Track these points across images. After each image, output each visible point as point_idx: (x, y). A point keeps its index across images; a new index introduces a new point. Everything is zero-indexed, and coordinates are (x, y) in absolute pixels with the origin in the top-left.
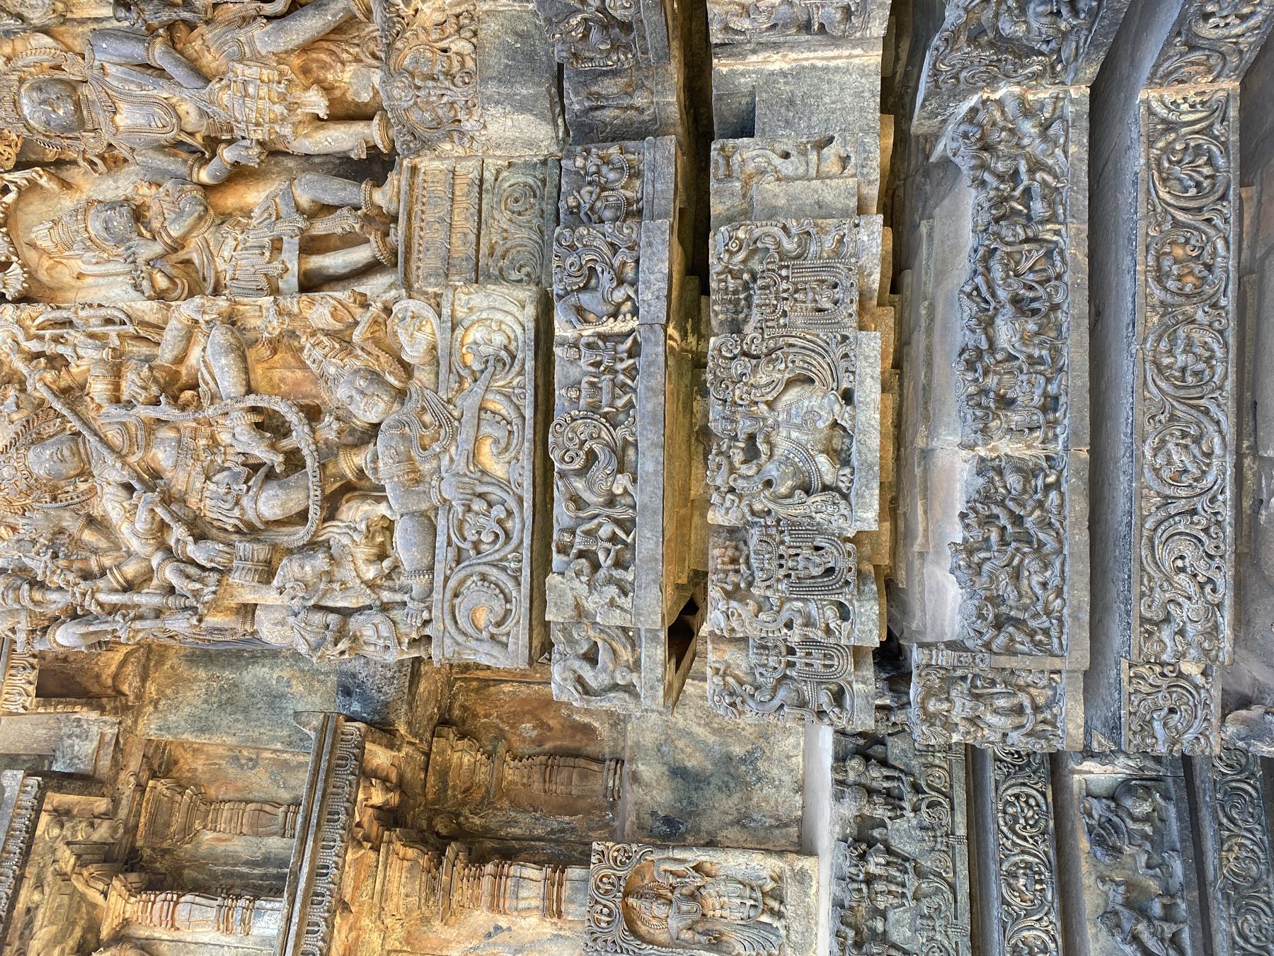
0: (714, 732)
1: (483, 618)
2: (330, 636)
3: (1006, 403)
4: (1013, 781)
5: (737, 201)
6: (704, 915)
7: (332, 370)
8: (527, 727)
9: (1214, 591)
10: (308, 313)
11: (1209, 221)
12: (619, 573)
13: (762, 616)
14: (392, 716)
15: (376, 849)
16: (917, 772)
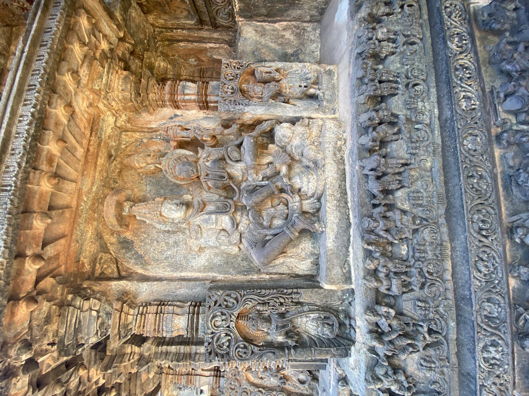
0: (279, 45)
8: (192, 61)
14: (112, 9)
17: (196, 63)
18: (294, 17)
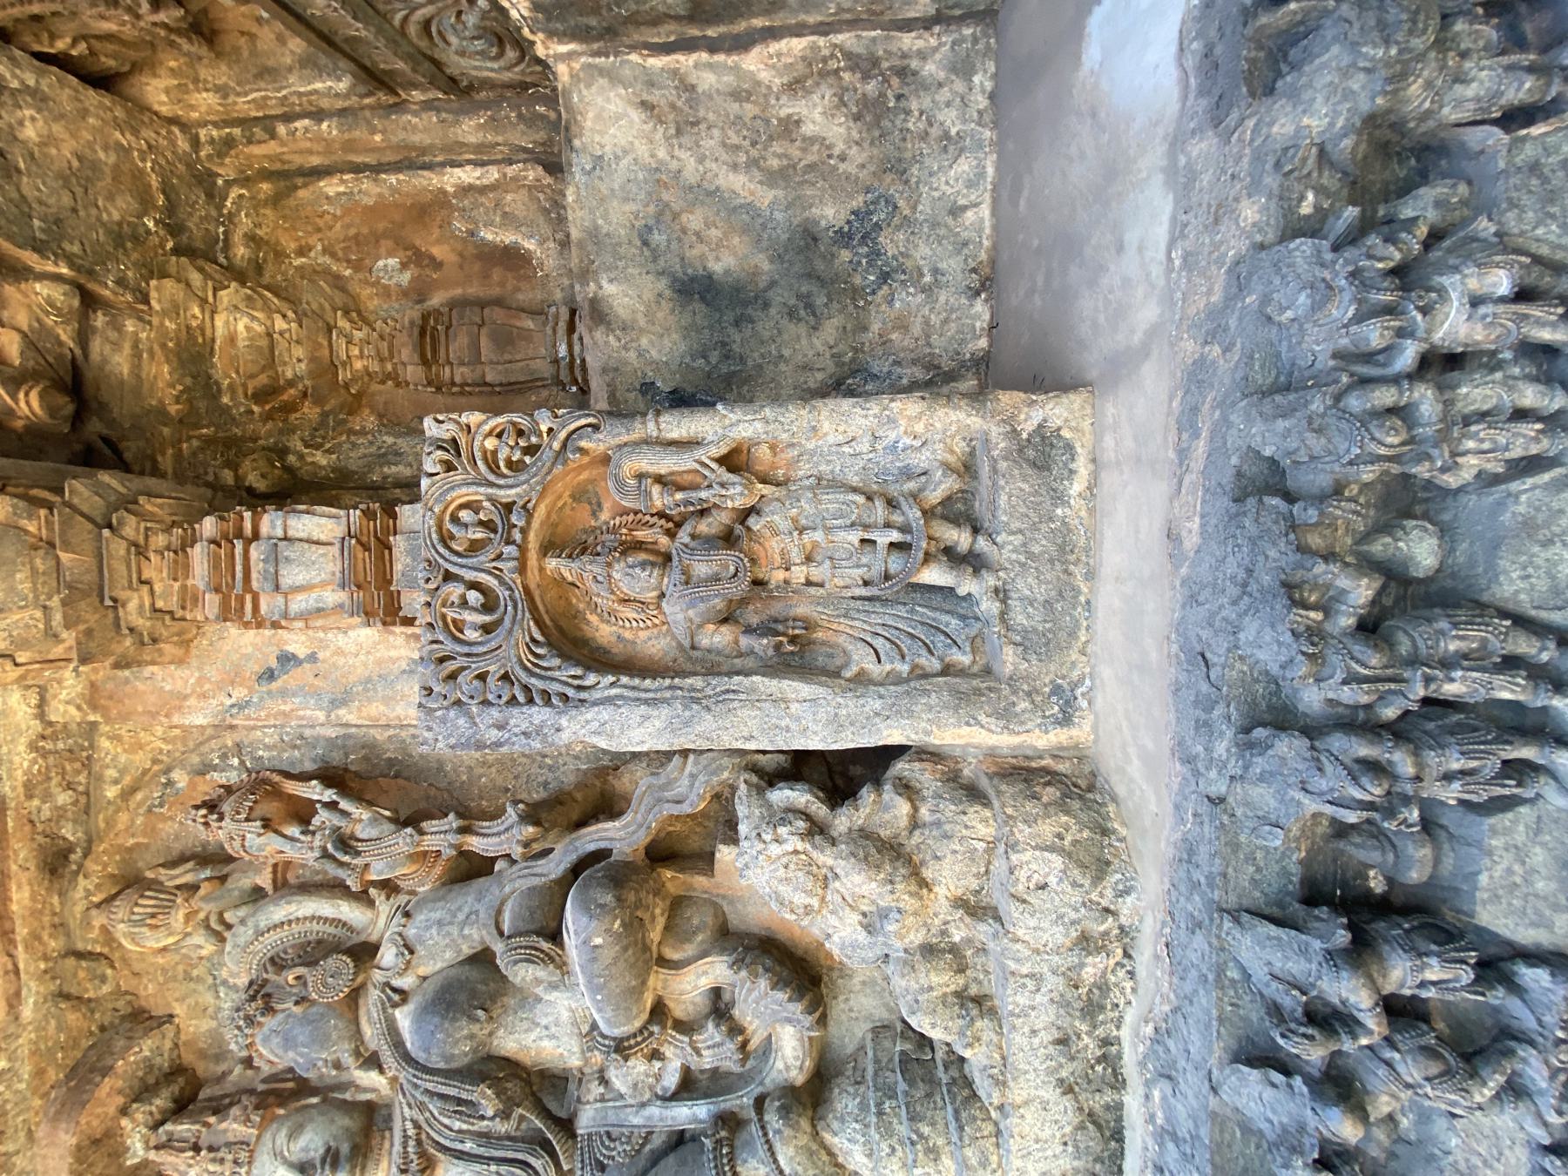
0: (772, 178)
6: (757, 583)
8: (388, 265)
17: (406, 278)
18: (840, 10)
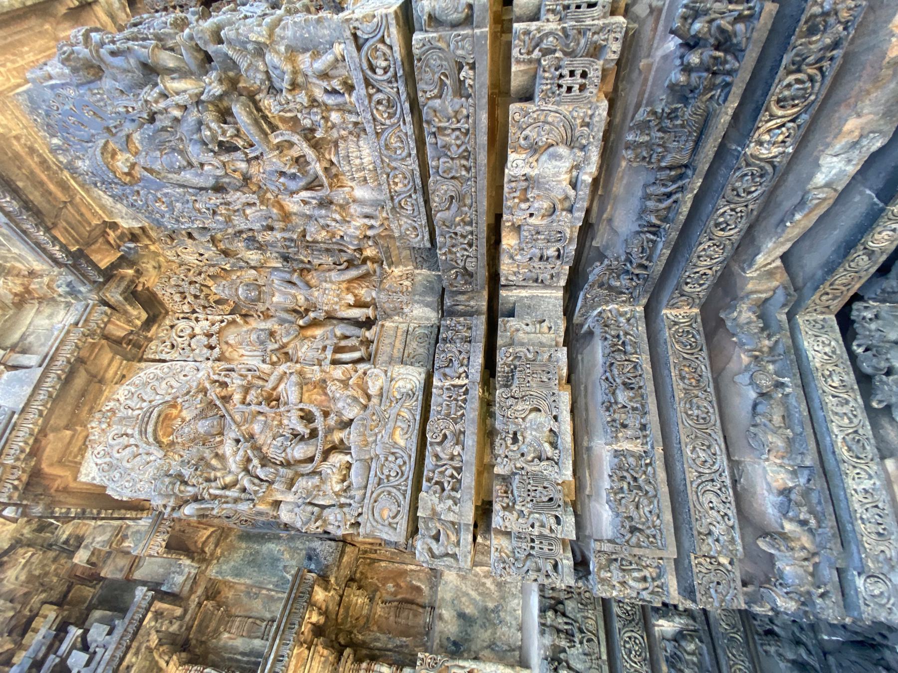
0: (479, 594)
1: (386, 514)
2: (313, 519)
3: (624, 426)
4: (627, 629)
5: (508, 340)
7: (338, 395)
8: (390, 586)
9: (729, 519)
10: (332, 372)
11: (697, 358)
12: (453, 494)
13: (520, 520)
15: (309, 649)
16: (580, 621)
17: (393, 590)
